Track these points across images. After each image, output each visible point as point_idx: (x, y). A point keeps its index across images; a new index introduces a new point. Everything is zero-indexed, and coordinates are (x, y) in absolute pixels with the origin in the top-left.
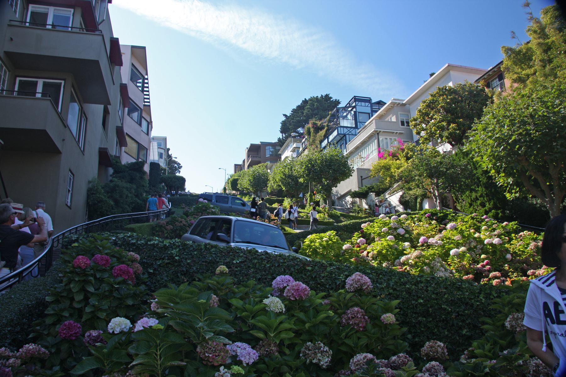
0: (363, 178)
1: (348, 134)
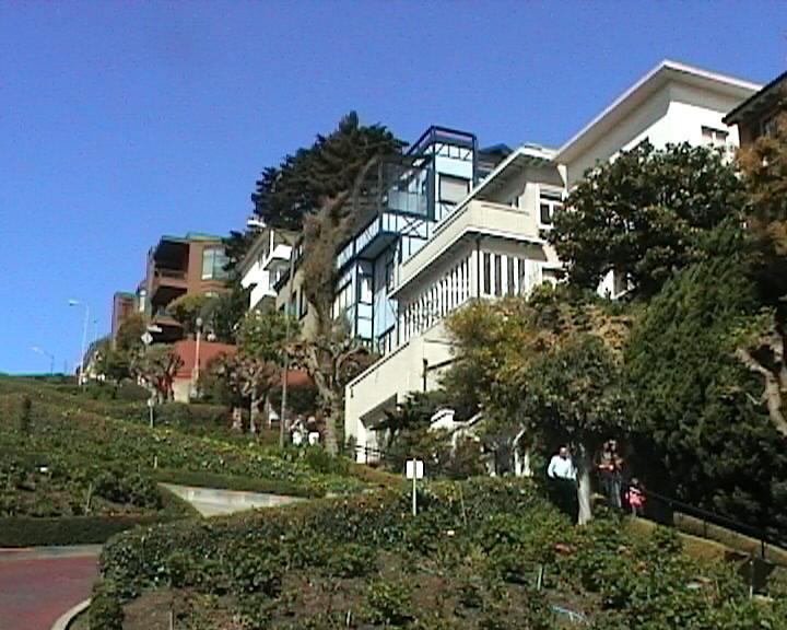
0: (429, 365)
1: (406, 235)
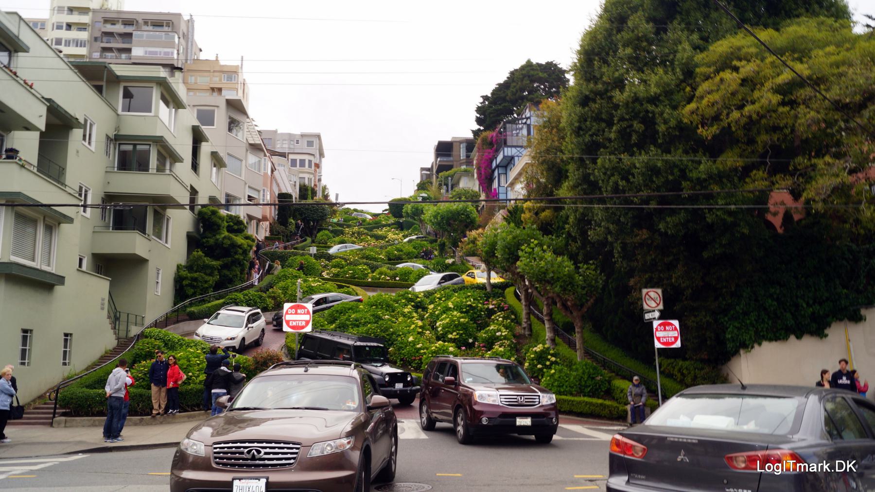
1: (517, 156)
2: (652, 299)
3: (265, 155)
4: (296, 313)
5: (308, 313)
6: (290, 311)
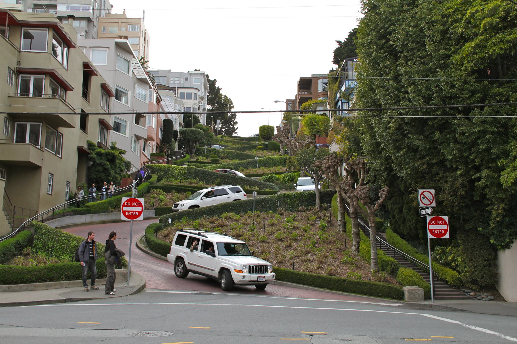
2: (426, 198)
3: (150, 88)
4: (131, 206)
5: (141, 205)
6: (126, 204)
